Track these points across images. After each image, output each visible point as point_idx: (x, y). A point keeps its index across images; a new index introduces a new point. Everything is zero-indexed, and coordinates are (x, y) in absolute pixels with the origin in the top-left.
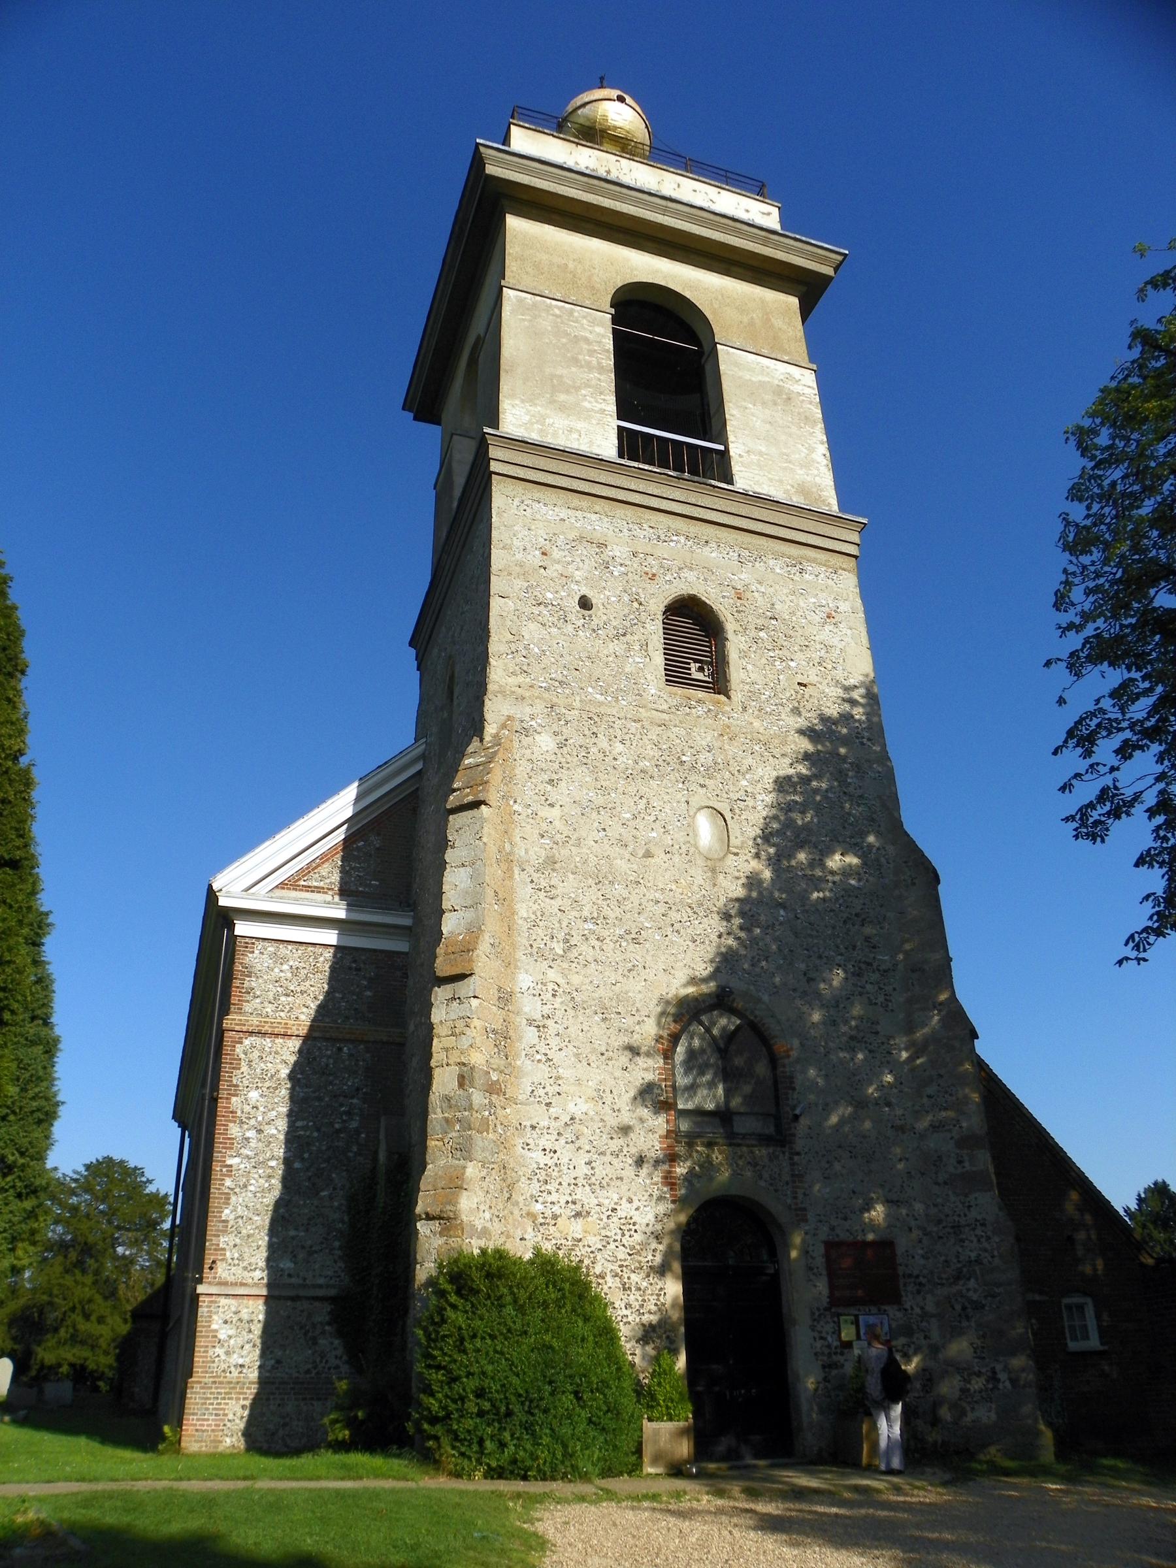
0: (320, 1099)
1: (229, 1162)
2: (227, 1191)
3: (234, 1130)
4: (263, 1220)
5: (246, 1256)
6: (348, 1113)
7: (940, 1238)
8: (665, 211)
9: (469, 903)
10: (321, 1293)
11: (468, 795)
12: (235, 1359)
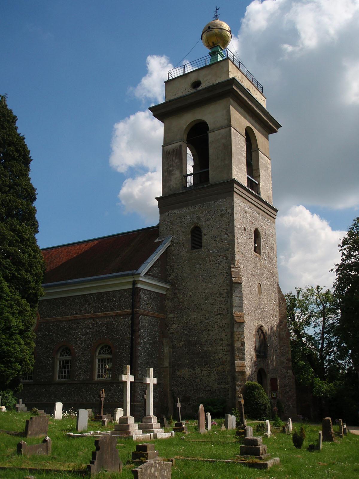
6: (157, 336)
7: (282, 378)
8: (257, 107)
9: (239, 305)
11: (238, 280)
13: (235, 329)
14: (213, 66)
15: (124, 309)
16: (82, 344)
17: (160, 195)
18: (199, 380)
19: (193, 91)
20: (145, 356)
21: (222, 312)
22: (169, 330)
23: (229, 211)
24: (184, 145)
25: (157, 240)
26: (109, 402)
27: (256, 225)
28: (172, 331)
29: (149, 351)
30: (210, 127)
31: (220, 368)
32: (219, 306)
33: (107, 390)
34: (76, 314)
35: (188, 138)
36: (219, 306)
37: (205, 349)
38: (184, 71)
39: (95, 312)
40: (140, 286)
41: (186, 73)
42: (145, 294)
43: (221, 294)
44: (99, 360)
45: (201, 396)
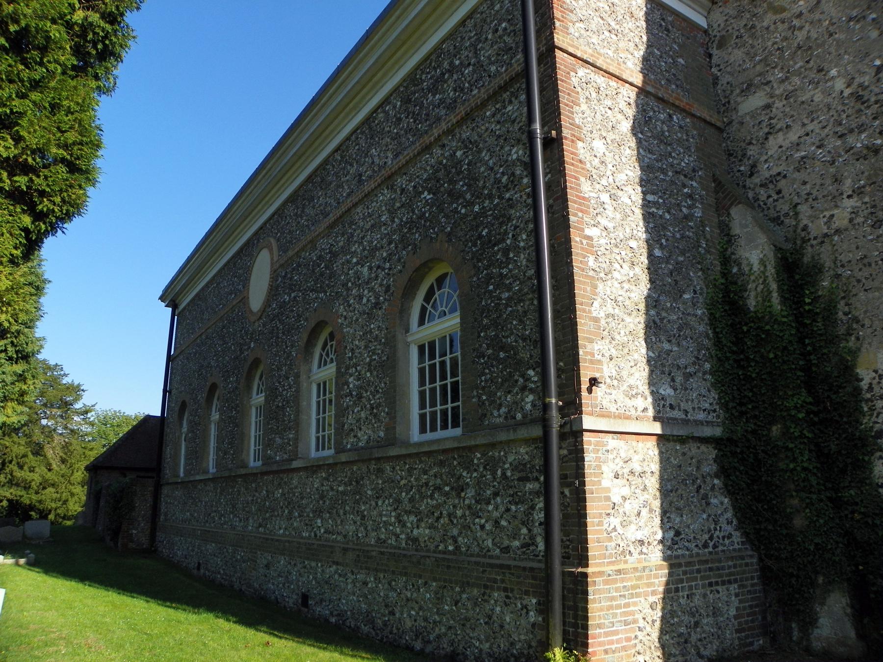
0: (663, 171)
1: (588, 232)
2: (591, 273)
3: (586, 187)
4: (637, 322)
5: (624, 373)
10: (707, 432)
12: (633, 533)
22: (751, 175)
33: (447, 489)
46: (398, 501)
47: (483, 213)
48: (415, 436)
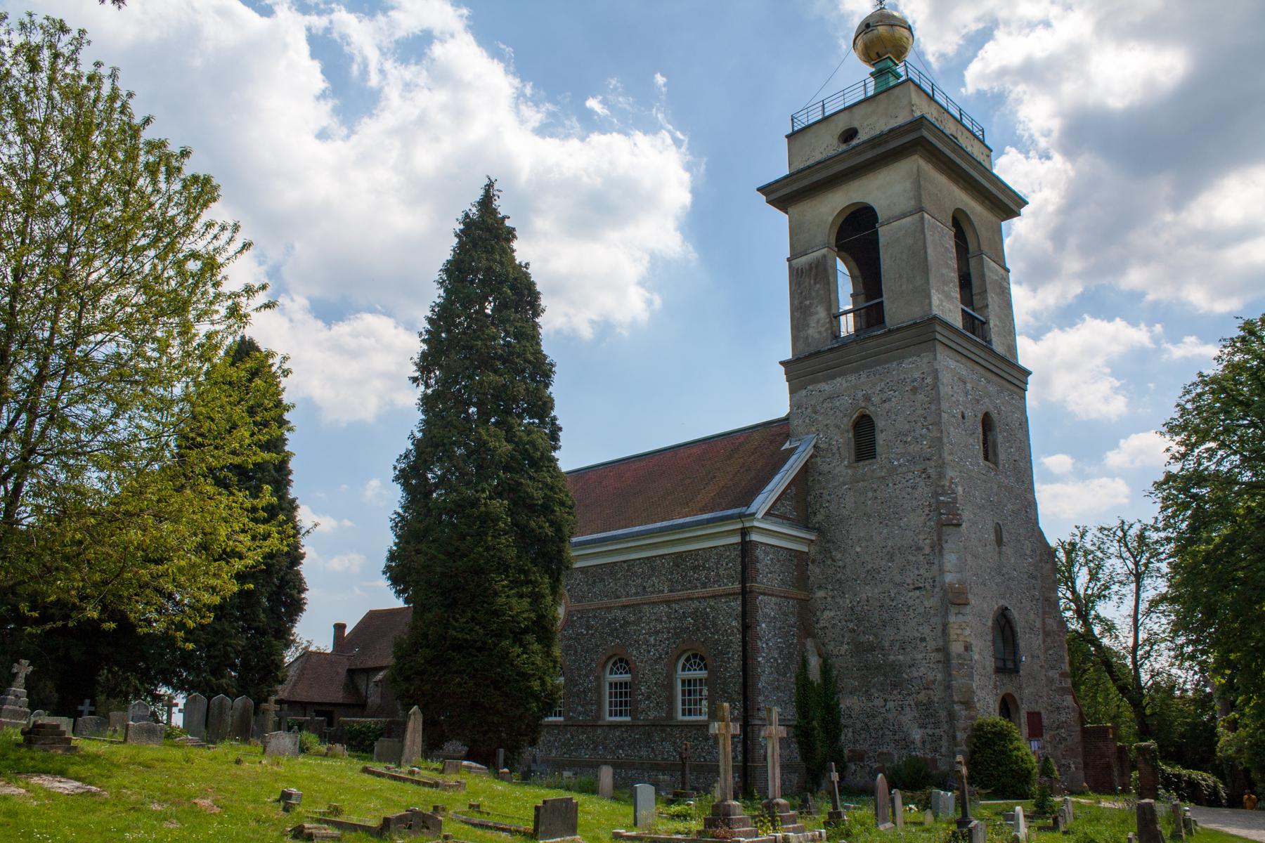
10: (791, 723)
13: (952, 619)
14: (881, 96)
15: (726, 585)
16: (649, 652)
17: (788, 355)
18: (880, 719)
19: (844, 147)
20: (772, 673)
21: (922, 585)
23: (929, 380)
24: (833, 254)
25: (787, 446)
26: (705, 760)
27: (987, 405)
28: (822, 623)
29: (778, 664)
30: (882, 215)
31: (922, 697)
32: (916, 572)
34: (636, 594)
35: (837, 240)
36: (916, 572)
37: (892, 658)
38: (824, 112)
39: (671, 591)
40: (755, 537)
41: (827, 114)
42: (767, 554)
43: (919, 549)
44: (683, 681)
45: (885, 751)
46: (675, 743)
47: (719, 640)
48: (680, 717)
